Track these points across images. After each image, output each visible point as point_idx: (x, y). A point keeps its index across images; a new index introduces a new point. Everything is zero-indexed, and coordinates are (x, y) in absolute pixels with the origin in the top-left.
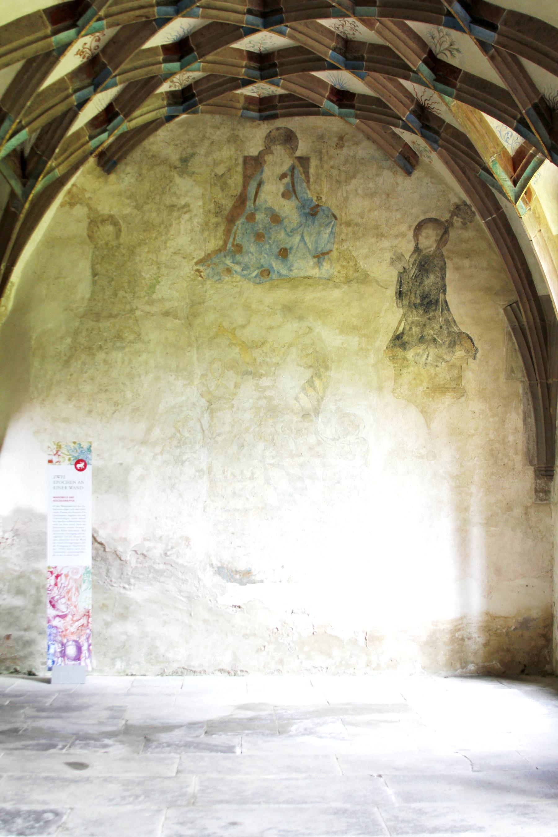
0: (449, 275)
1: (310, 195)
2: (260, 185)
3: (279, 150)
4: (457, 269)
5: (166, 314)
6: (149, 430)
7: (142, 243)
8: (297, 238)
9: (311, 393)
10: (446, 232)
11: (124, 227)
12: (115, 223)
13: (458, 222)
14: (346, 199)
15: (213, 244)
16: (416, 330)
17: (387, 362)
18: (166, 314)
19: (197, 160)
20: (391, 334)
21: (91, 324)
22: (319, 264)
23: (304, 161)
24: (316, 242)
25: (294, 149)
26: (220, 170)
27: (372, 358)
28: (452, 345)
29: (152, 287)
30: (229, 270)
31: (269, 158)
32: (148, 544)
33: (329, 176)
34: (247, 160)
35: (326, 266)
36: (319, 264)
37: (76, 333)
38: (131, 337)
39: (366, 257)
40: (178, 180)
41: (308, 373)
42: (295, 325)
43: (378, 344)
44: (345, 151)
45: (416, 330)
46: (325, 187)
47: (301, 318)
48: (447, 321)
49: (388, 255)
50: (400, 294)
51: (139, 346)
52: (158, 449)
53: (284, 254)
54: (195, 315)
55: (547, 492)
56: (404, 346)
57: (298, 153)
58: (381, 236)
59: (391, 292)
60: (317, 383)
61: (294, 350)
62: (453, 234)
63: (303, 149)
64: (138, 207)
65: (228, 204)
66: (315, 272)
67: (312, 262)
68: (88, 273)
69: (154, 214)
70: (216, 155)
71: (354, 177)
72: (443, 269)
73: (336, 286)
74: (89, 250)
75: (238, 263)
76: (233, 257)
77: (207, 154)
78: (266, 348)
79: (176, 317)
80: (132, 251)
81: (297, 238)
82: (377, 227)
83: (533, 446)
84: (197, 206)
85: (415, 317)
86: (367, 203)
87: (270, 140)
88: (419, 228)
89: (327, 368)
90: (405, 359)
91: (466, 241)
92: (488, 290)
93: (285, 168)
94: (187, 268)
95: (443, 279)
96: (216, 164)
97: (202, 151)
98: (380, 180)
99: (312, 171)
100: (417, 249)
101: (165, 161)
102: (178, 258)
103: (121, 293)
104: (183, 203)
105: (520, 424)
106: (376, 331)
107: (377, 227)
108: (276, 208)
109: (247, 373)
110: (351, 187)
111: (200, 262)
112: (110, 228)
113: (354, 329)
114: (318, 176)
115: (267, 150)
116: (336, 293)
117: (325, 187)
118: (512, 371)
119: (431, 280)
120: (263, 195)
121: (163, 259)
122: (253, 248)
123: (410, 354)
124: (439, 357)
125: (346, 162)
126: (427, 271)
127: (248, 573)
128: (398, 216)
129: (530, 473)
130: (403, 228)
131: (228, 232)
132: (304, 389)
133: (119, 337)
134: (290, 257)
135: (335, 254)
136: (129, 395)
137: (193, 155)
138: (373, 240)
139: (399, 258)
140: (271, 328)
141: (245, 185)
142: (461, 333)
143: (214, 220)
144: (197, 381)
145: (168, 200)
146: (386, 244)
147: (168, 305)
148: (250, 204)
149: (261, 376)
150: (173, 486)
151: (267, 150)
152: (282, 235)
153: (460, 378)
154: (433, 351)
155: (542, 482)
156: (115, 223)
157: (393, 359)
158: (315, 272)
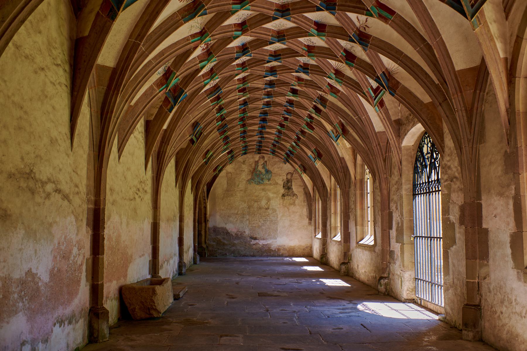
0: (293, 183)
1: (267, 168)
2: (258, 166)
3: (261, 160)
4: (294, 182)
5: (241, 190)
6: (238, 212)
7: (236, 177)
8: (265, 177)
9: (267, 205)
10: (292, 175)
11: (233, 174)
12: (231, 174)
13: (294, 173)
14: (274, 169)
15: (249, 177)
16: (286, 193)
17: (281, 199)
18: (241, 190)
19: (246, 161)
20: (282, 194)
21: (227, 192)
22: (269, 181)
23: (266, 162)
24: (268, 177)
25: (264, 159)
26: (250, 163)
27: (278, 199)
28: (293, 196)
29: (238, 186)
30: (252, 182)
31: (260, 161)
32: (238, 233)
33: (271, 165)
34: (255, 161)
35: (270, 181)
36: (269, 181)
37: (224, 194)
38: (234, 195)
39: (277, 180)
40: (243, 165)
41: (267, 201)
42: (264, 192)
43: (279, 196)
44: (274, 160)
45: (286, 193)
46: (270, 166)
47: (265, 191)
48: (292, 192)
49: (281, 179)
50: (284, 187)
51: (236, 196)
52: (239, 215)
53: (262, 179)
54: (246, 191)
55: (311, 223)
56: (284, 196)
57: (265, 160)
58: (280, 176)
59: (282, 186)
60: (268, 203)
61: (264, 197)
62: (294, 175)
63: (266, 159)
64: (235, 171)
65: (252, 170)
66: (268, 183)
67: (267, 181)
68: (226, 183)
69: (238, 172)
70: (250, 161)
71: (275, 164)
72: (292, 182)
73: (272, 185)
74: (226, 179)
75: (254, 181)
76: (253, 180)
77: (248, 160)
78: (259, 197)
79: (242, 191)
80: (234, 179)
81: (265, 177)
82: (279, 174)
83: (308, 215)
84: (246, 170)
85: (286, 191)
86: (278, 169)
87: (260, 158)
88: (287, 174)
89: (270, 200)
90: (285, 199)
91: (296, 177)
92: (300, 186)
93: (263, 163)
94: (244, 182)
95: (292, 184)
96: (250, 162)
97: (247, 160)
98: (280, 165)
99: (268, 163)
100: (287, 178)
101: (240, 162)
102: (243, 180)
103: (232, 187)
104: (244, 169)
105: (306, 211)
106: (279, 193)
107: (279, 174)
108: (261, 170)
109: (256, 201)
110: (275, 167)
111: (247, 181)
112: (230, 174)
113: (275, 193)
114: (269, 164)
115: (259, 160)
116: (272, 187)
117: (270, 166)
118: (304, 201)
119: (289, 184)
120: (258, 168)
121: (240, 180)
122: (257, 178)
123: (285, 198)
124: (291, 198)
125: (274, 162)
126: (289, 182)
127: (256, 238)
128: (283, 172)
129: (308, 219)
130: (284, 174)
131: (252, 175)
132: (266, 204)
133: (232, 195)
134: (264, 180)
135: (272, 179)
136: (234, 205)
137: (245, 160)
138: (279, 177)
139: (284, 180)
140: (260, 193)
141: (255, 166)
142: (295, 194)
143: (249, 173)
144: (246, 203)
145: (241, 169)
146: (281, 177)
147: (241, 189)
148: (256, 170)
149: (258, 202)
150: (242, 222)
151: (259, 160)
152: (262, 176)
153: (295, 202)
154: (290, 197)
155: (310, 221)
156: (231, 174)
157: (282, 198)
158: (268, 183)
